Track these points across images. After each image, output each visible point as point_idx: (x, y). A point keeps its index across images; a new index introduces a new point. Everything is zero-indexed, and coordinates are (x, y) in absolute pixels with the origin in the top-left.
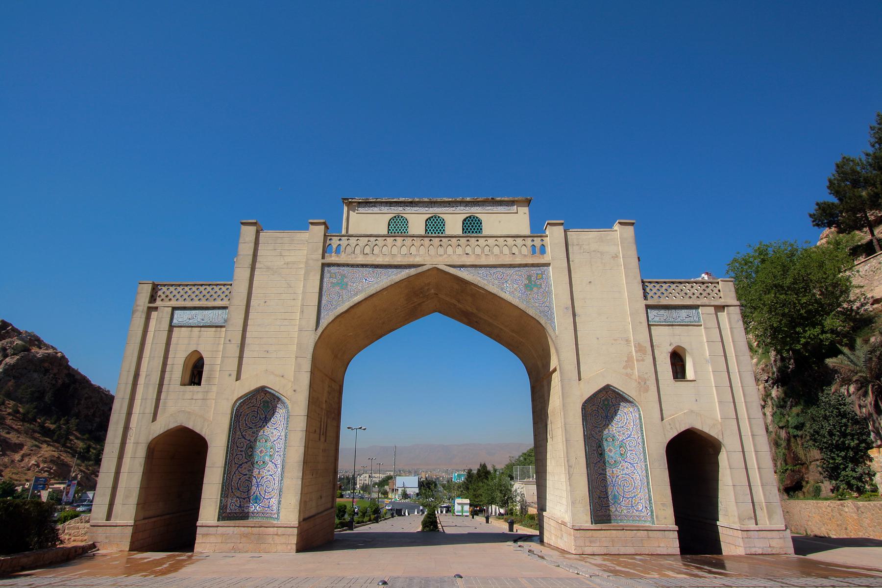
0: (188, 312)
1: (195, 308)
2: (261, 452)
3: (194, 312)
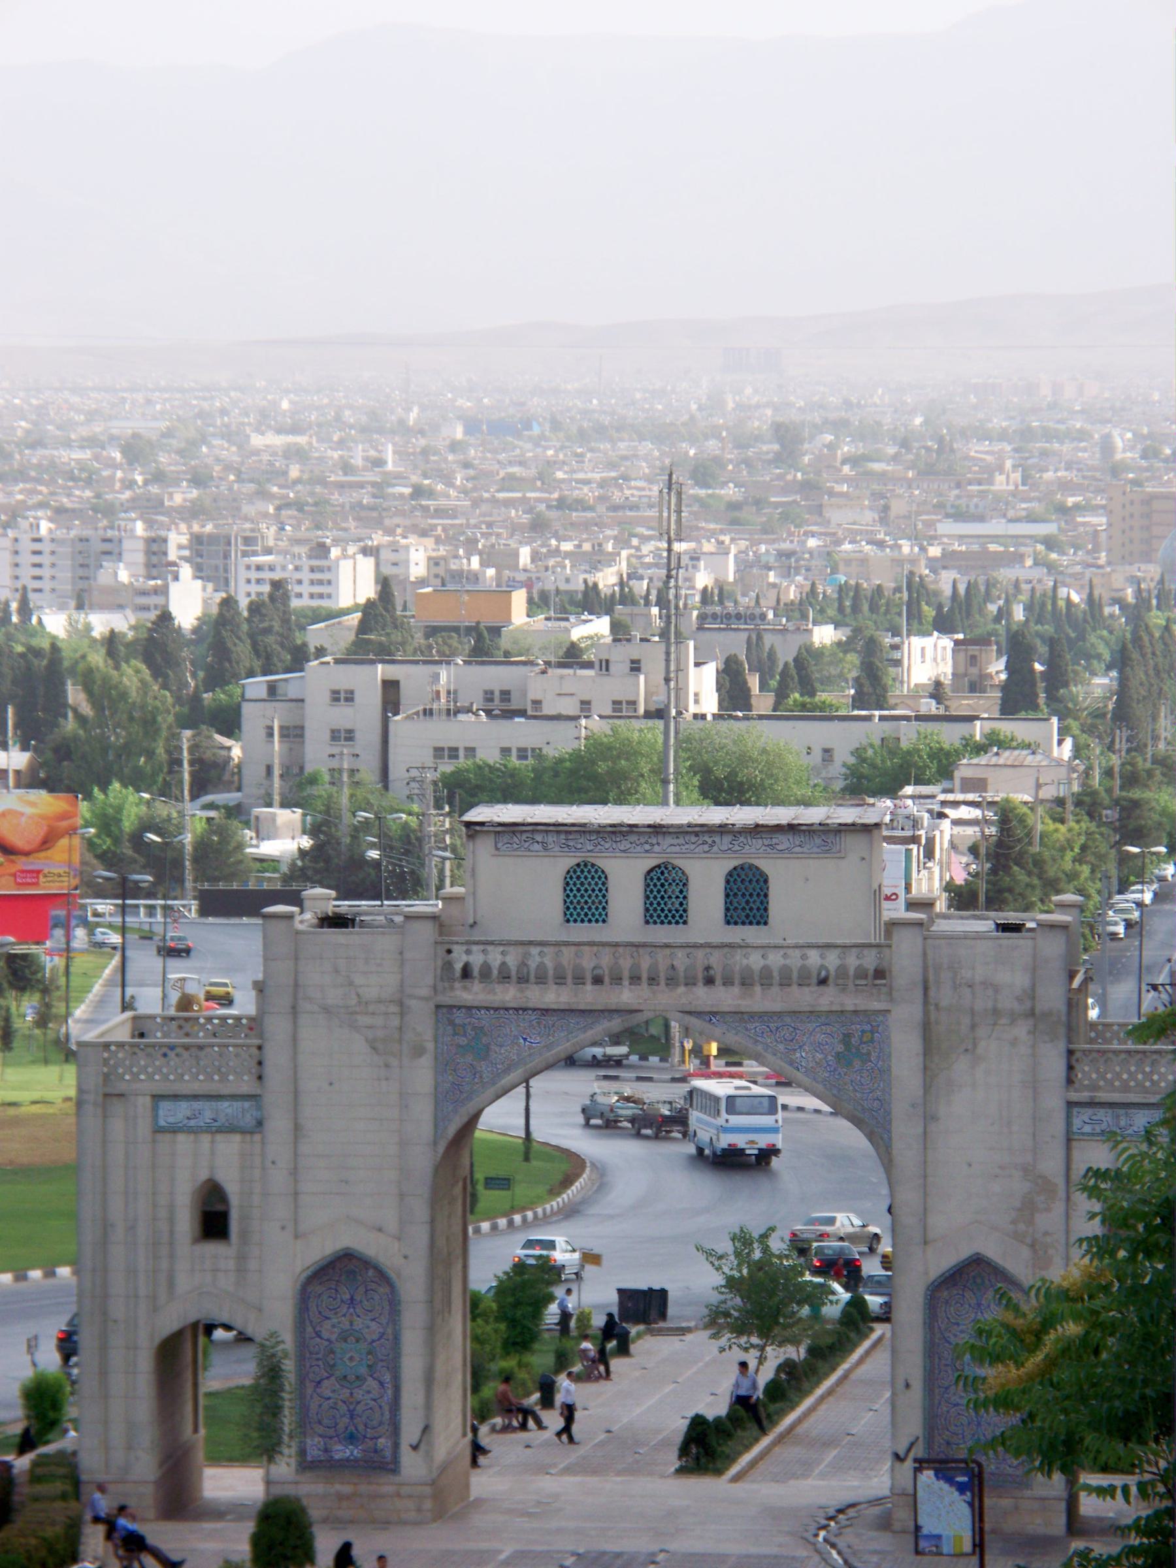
0: (184, 1105)
1: (196, 1097)
2: (351, 1359)
3: (197, 1105)
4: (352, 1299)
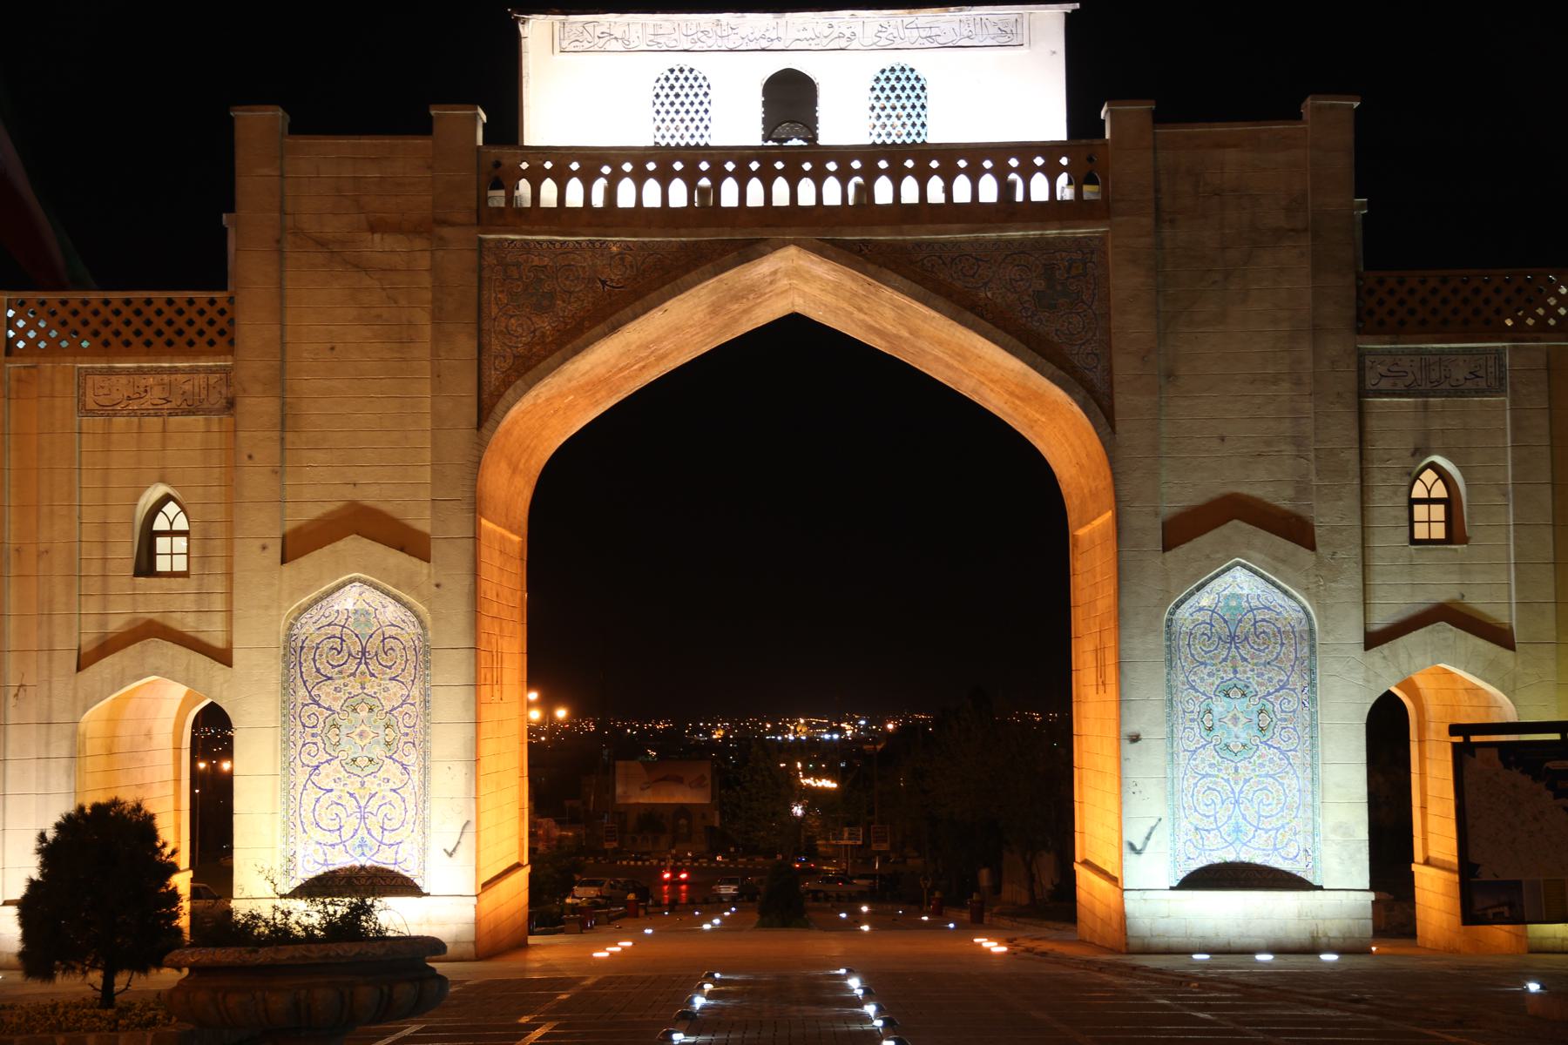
0: (123, 380)
2: (361, 735)
4: (364, 652)
